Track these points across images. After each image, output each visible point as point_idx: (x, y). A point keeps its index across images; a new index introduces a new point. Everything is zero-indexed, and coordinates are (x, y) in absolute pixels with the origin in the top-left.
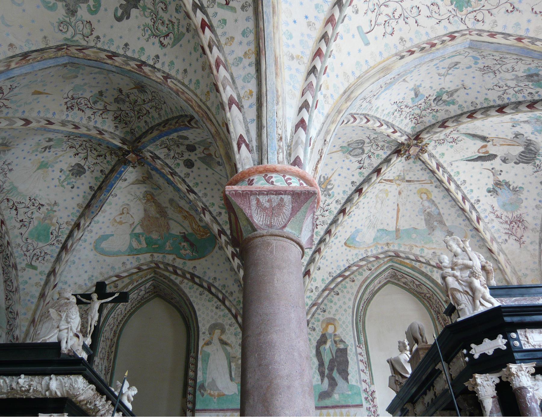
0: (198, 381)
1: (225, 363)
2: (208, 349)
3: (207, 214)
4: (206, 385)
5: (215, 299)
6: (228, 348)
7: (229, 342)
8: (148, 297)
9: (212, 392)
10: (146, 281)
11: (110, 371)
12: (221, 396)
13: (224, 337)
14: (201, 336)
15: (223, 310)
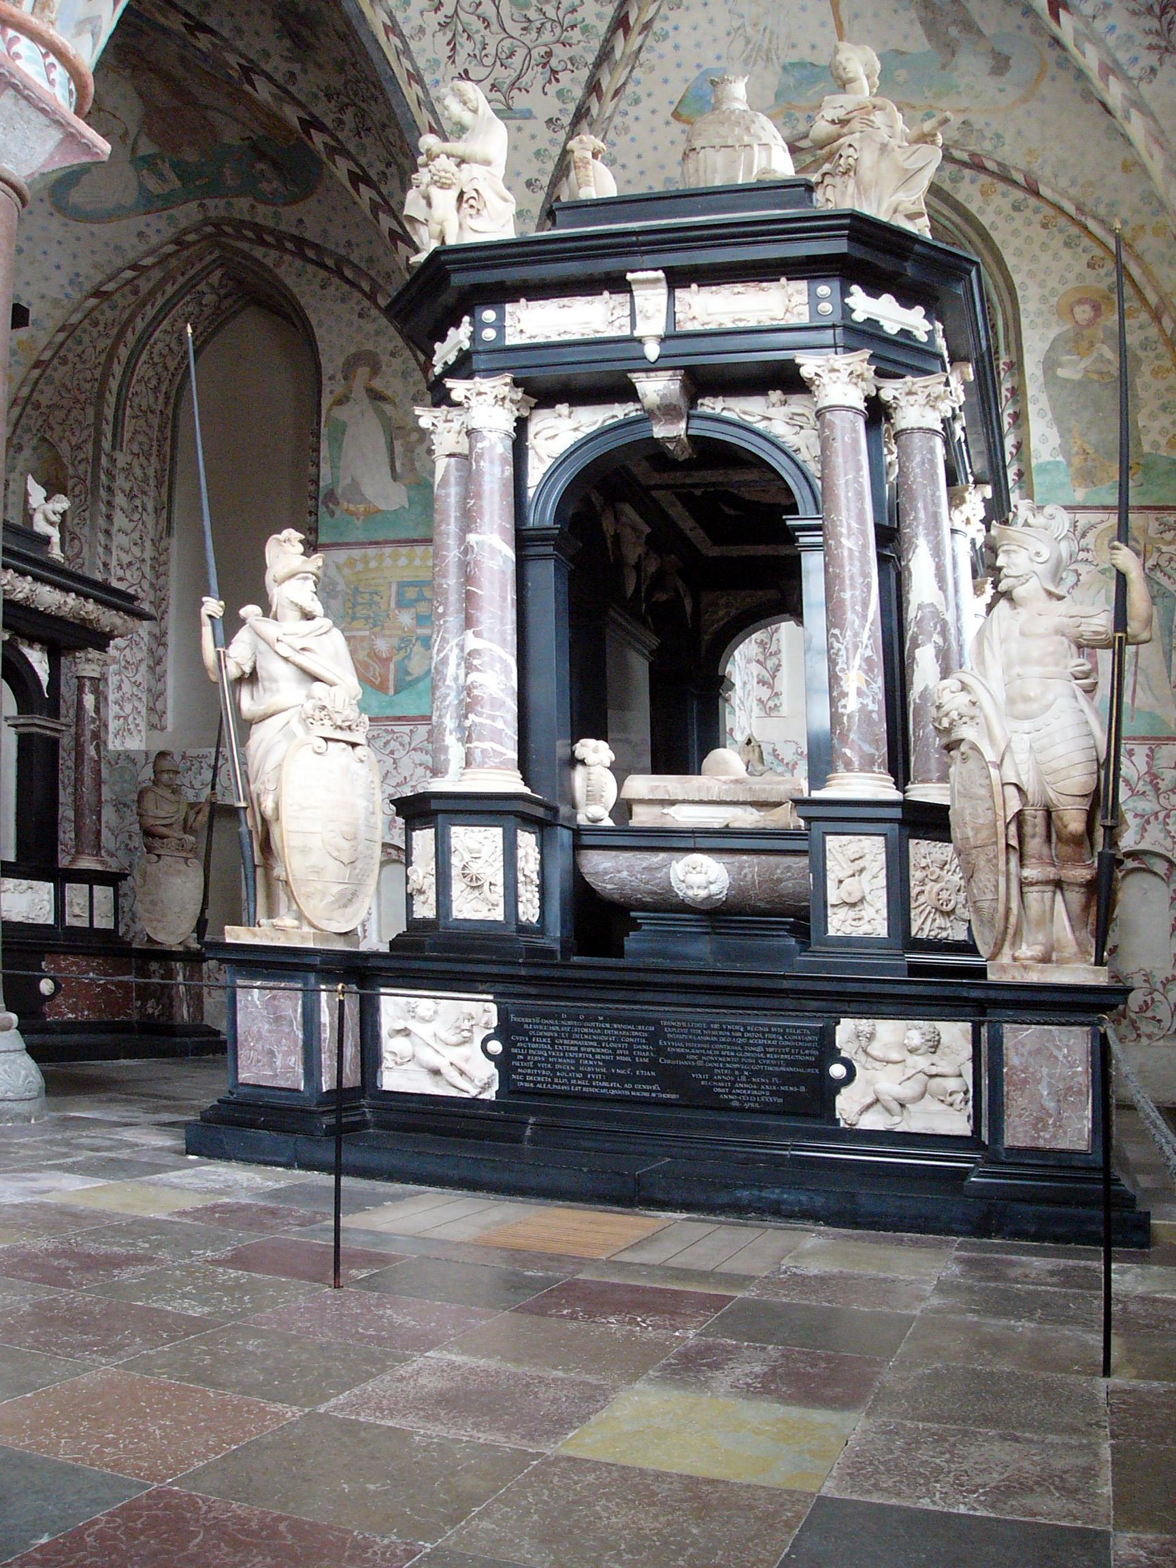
0: (322, 484)
1: (382, 442)
2: (341, 413)
3: (260, 82)
4: (339, 491)
5: (358, 295)
6: (387, 408)
7: (389, 393)
8: (231, 307)
9: (352, 507)
10: (206, 272)
11: (166, 478)
12: (372, 514)
13: (377, 384)
14: (327, 386)
15: (374, 320)
